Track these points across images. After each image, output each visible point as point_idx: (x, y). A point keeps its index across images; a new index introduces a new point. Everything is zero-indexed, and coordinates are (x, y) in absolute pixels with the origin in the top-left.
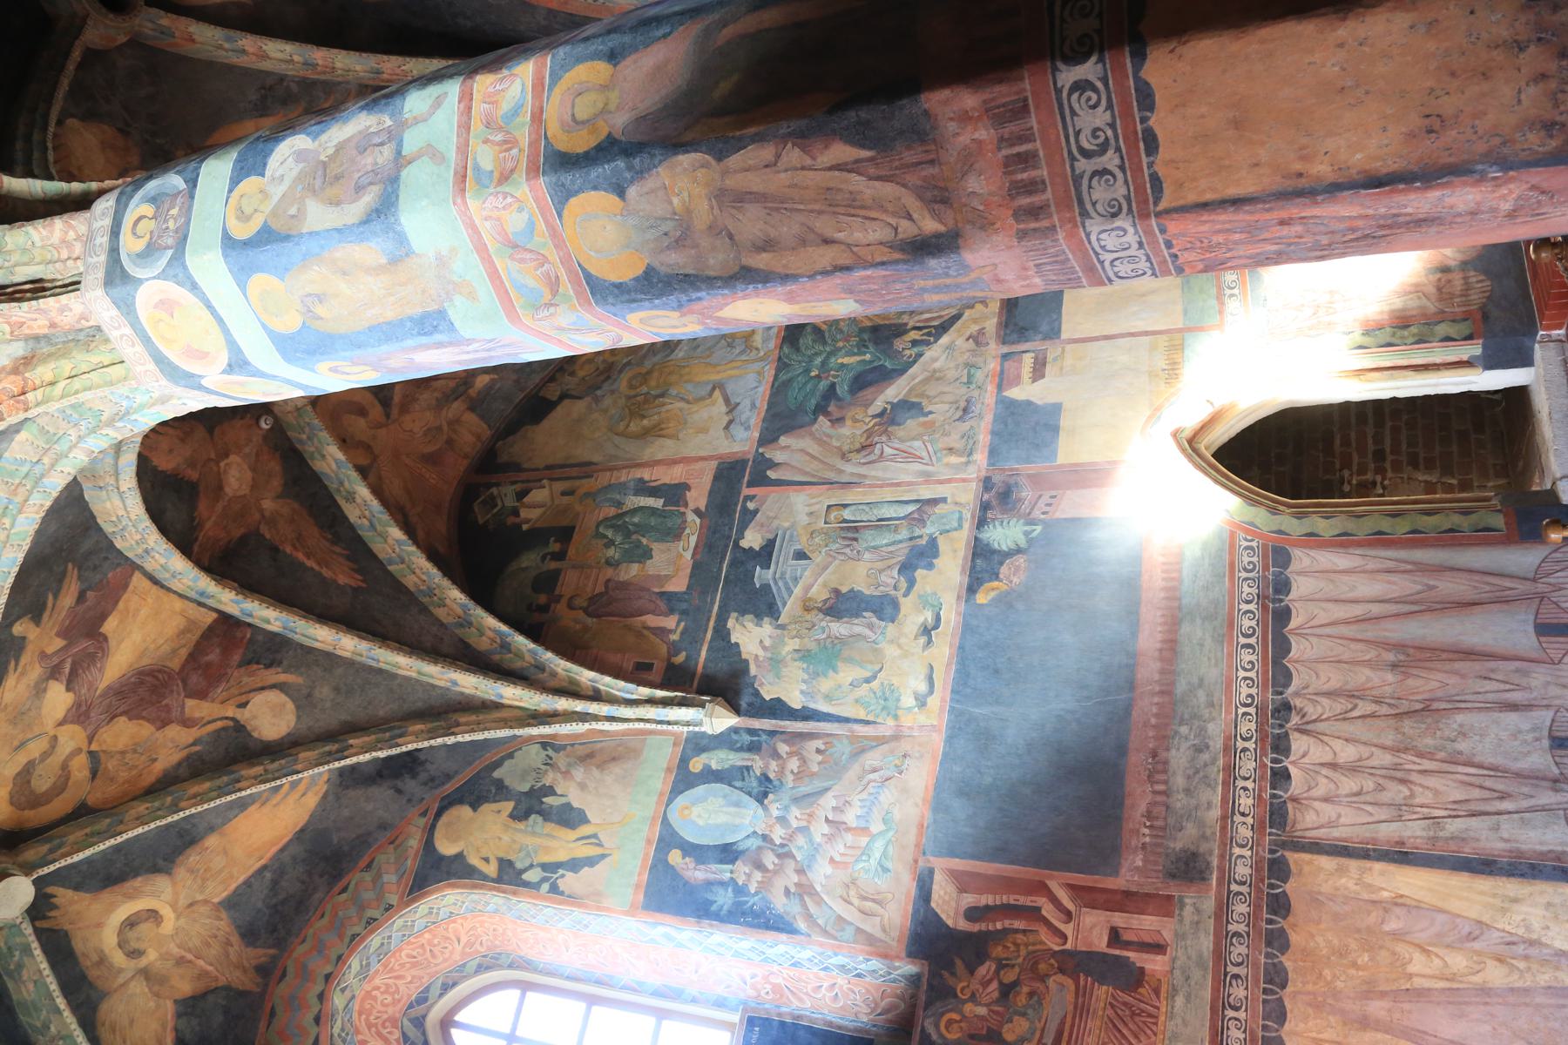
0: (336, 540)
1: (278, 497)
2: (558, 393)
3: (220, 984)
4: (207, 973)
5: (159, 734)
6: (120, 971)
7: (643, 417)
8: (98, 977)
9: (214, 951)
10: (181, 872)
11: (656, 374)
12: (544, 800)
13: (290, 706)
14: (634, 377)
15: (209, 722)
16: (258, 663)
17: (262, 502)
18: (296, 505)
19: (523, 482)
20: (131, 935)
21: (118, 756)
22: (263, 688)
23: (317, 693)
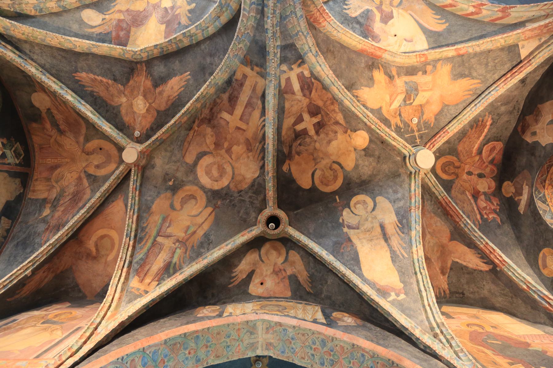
0: (92, 94)
1: (121, 105)
5: (128, 7)
13: (86, 21)
15: (113, 12)
17: (126, 100)
18: (113, 103)
19: (4, 164)
22: (100, 25)
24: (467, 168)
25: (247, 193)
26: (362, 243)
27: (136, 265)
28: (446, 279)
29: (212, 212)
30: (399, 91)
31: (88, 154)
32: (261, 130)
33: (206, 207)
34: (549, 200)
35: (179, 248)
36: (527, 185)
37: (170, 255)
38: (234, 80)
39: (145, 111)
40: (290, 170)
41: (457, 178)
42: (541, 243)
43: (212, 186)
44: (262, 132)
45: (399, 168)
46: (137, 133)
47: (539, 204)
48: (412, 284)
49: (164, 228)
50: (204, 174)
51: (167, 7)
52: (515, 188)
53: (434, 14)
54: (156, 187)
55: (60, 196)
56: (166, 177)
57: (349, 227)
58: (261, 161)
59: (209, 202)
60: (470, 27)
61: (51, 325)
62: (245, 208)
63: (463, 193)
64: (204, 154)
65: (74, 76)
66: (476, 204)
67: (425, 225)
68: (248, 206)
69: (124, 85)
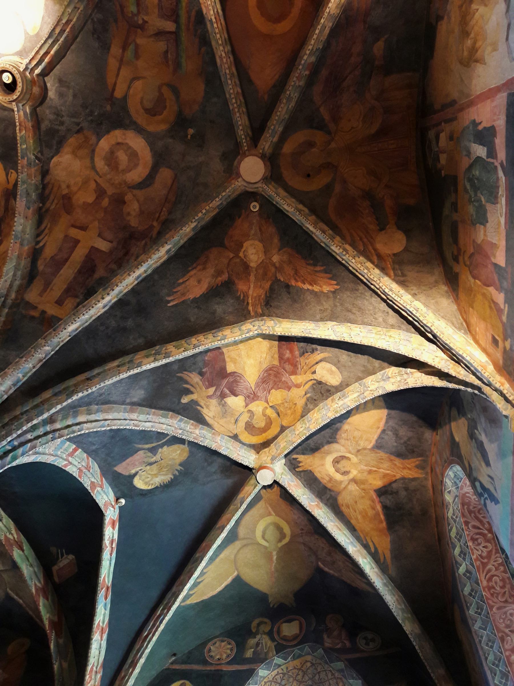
1: (279, 250)
3: (397, 478)
4: (388, 474)
5: (290, 393)
6: (341, 482)
8: (332, 486)
9: (386, 465)
10: (342, 441)
12: (476, 431)
13: (334, 368)
15: (306, 383)
16: (307, 352)
17: (273, 259)
20: (339, 466)
22: (317, 363)
23: (342, 360)
25: (69, 130)
29: (114, 90)
32: (45, 228)
33: (125, 98)
35: (136, 15)
38: (81, 297)
39: (245, 245)
40: (7, 175)
43: (124, 134)
44: (43, 227)
46: (255, 207)
50: (140, 153)
51: (233, 398)
58: (49, 183)
59: (125, 108)
62: (68, 103)
68: (63, 108)
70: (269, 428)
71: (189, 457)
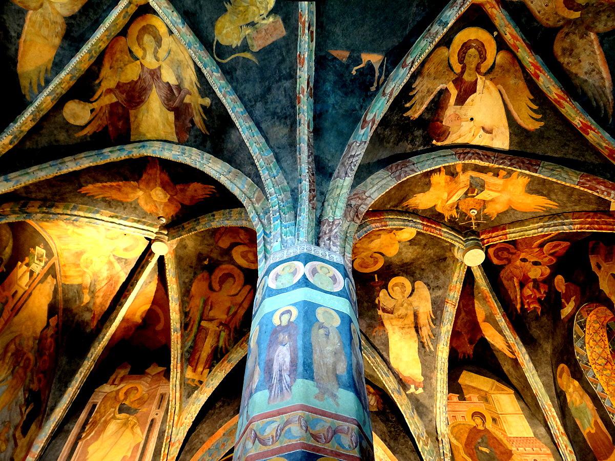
1: (138, 198)
2: (51, 324)
5: (117, 80)
7: (12, 355)
10: (60, 20)
11: (22, 375)
13: (72, 121)
14: (29, 362)
15: (100, 96)
18: (129, 200)
21: (127, 63)
22: (89, 123)
23: (65, 134)
24: (522, 256)
26: (394, 329)
27: (187, 354)
28: (473, 347)
30: (462, 185)
31: (112, 239)
33: (245, 285)
34: (587, 327)
36: (574, 300)
37: (216, 340)
41: (508, 264)
42: (565, 358)
45: (446, 251)
47: (576, 328)
48: (431, 378)
49: (206, 312)
52: (566, 290)
53: (531, 100)
54: (191, 267)
55: (95, 281)
56: (200, 257)
57: (384, 310)
60: (569, 141)
61: (128, 415)
63: (511, 279)
64: (240, 244)
65: (80, 192)
66: (521, 292)
67: (461, 305)
69: (137, 180)
70: (139, 31)
71: (217, 20)
